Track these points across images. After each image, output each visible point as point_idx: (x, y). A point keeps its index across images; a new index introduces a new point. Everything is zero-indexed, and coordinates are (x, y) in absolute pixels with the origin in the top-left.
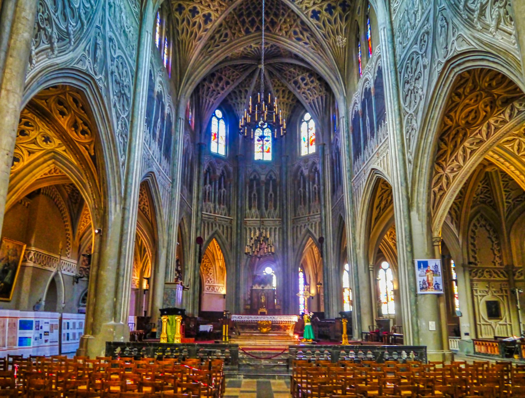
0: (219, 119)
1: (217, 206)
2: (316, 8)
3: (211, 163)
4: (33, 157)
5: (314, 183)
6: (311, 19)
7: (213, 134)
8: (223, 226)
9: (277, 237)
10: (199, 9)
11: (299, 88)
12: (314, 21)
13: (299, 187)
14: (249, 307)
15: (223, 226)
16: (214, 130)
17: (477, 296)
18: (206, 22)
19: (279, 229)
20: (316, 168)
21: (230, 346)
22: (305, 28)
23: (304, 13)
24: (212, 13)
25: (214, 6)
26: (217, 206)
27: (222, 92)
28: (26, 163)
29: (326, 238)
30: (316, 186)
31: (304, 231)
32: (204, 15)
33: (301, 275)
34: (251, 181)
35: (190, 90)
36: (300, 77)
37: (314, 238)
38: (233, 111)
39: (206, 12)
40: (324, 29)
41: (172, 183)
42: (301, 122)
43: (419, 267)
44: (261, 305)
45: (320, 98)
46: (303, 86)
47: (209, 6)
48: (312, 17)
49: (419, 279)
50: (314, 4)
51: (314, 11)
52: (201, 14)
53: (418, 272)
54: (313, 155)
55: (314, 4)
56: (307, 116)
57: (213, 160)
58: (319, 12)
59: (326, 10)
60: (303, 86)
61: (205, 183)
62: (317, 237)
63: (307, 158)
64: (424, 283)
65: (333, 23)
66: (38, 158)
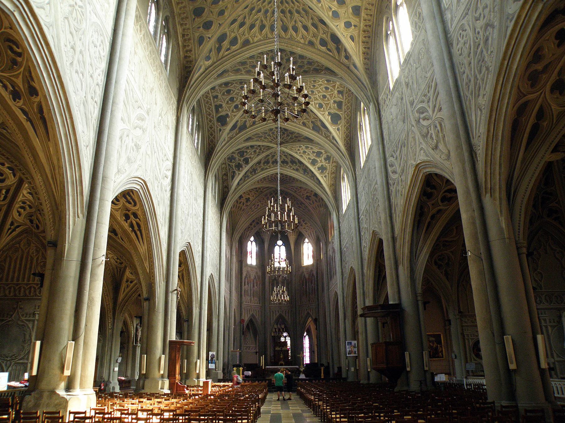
0: (252, 242)
1: (252, 299)
2: (308, 194)
3: (248, 271)
5: (312, 283)
6: (306, 200)
7: (248, 252)
8: (256, 311)
9: (290, 316)
10: (243, 196)
11: (301, 225)
12: (308, 201)
13: (303, 285)
14: (273, 361)
15: (256, 311)
16: (249, 249)
17: (468, 339)
18: (247, 202)
19: (291, 311)
20: (313, 274)
21: (268, 380)
22: (302, 203)
24: (250, 197)
25: (251, 194)
26: (252, 299)
27: (254, 228)
30: (313, 285)
31: (306, 312)
32: (246, 199)
33: (307, 338)
34: (273, 280)
35: (238, 238)
36: (302, 220)
37: (312, 318)
38: (260, 236)
39: (247, 197)
41: (230, 294)
42: (304, 243)
43: (348, 344)
44: (280, 359)
46: (304, 224)
47: (249, 194)
48: (306, 199)
49: (348, 350)
50: (307, 192)
51: (307, 196)
52: (244, 198)
53: (347, 347)
54: (313, 265)
55: (307, 192)
56: (307, 240)
57: (249, 269)
58: (310, 196)
59: (314, 195)
60: (304, 224)
61: (245, 285)
62: (314, 318)
63: (308, 267)
64: (350, 351)
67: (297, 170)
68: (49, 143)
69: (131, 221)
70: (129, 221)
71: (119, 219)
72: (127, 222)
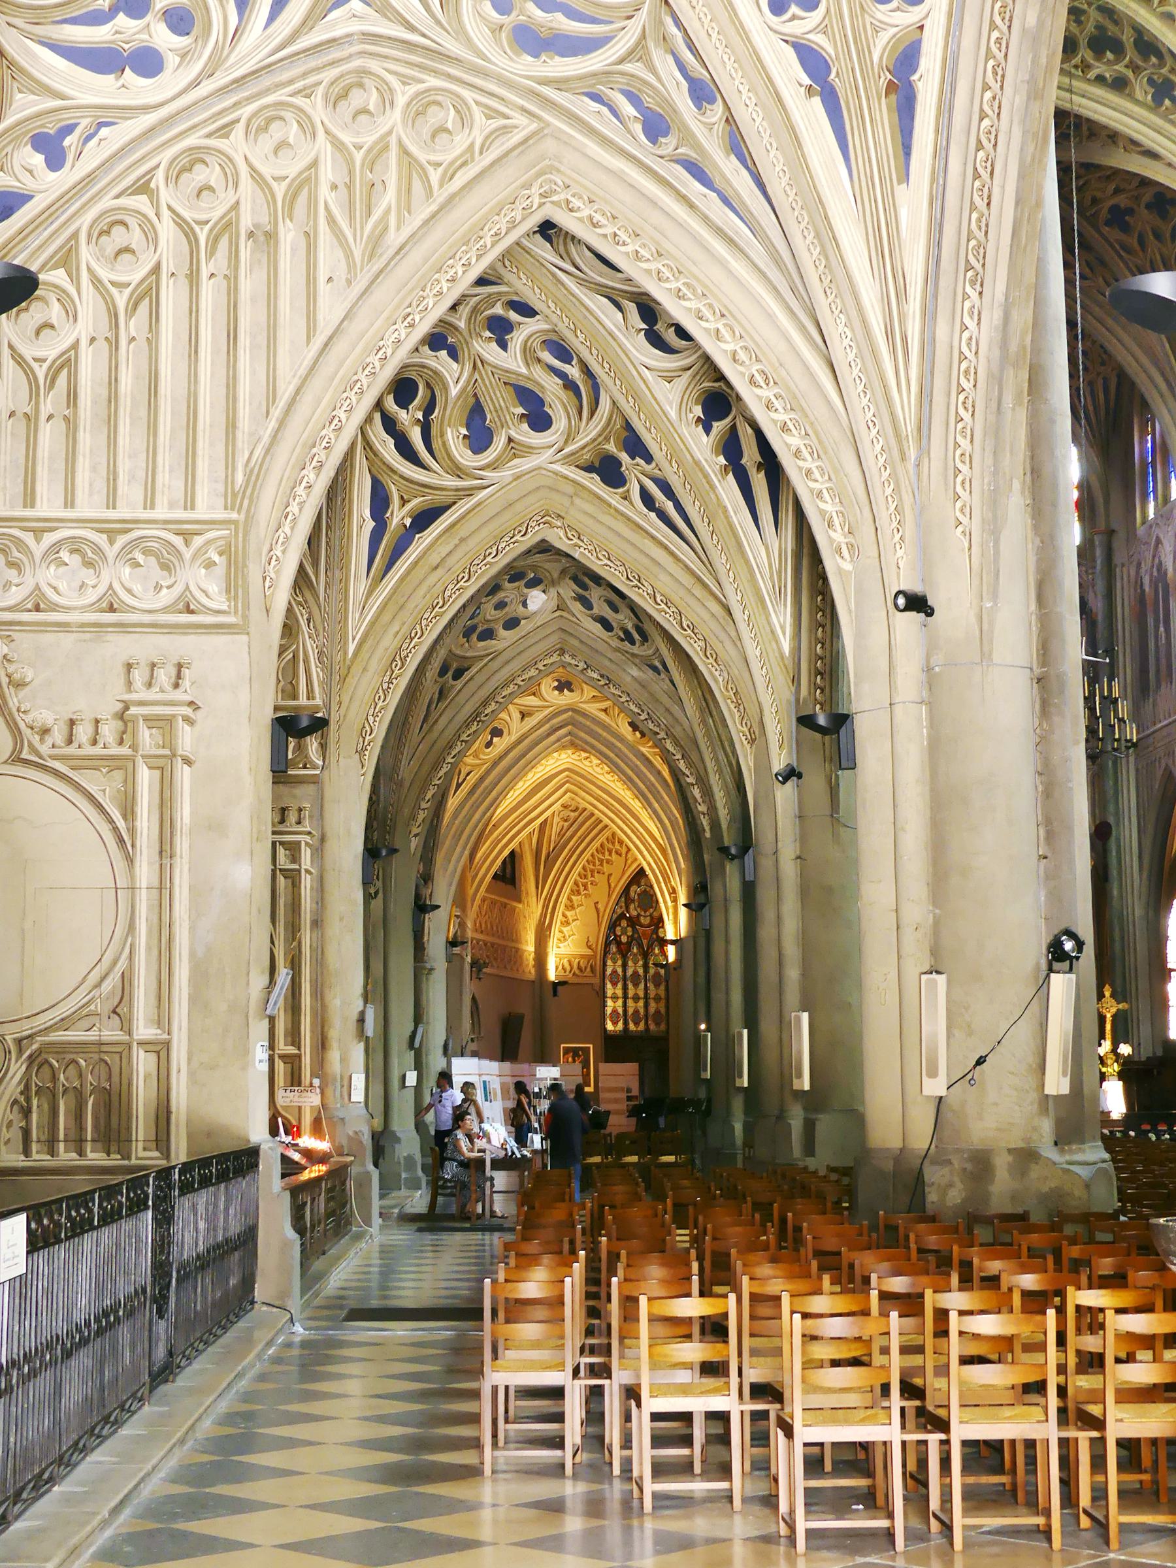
2: (1122, 201)
4: (531, 722)
6: (1106, 230)
12: (1114, 234)
23: (1088, 214)
28: (514, 738)
29: (1118, 824)
40: (1141, 253)
45: (1100, 382)
48: (1107, 223)
50: (1117, 191)
51: (1114, 209)
55: (1117, 191)
58: (1130, 211)
59: (1148, 206)
65: (1169, 239)
66: (540, 724)
67: (1119, 85)
68: (900, 190)
69: (733, 429)
70: (718, 426)
71: (673, 414)
72: (708, 430)
